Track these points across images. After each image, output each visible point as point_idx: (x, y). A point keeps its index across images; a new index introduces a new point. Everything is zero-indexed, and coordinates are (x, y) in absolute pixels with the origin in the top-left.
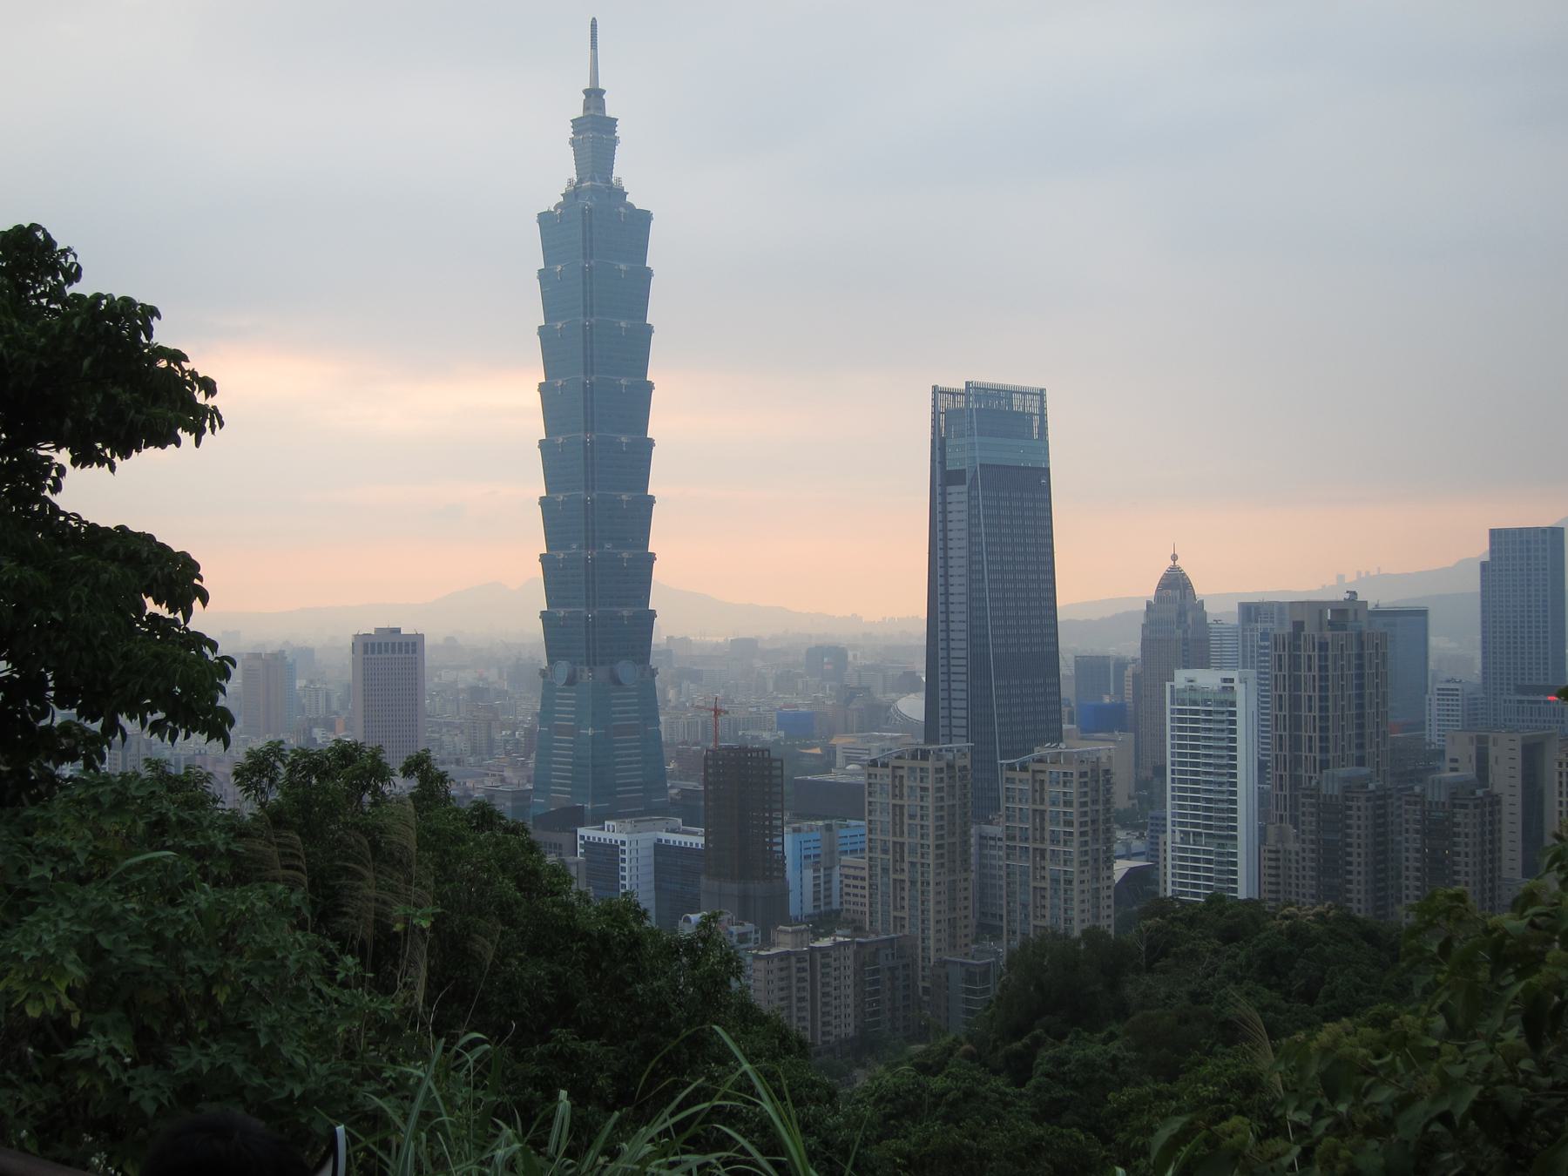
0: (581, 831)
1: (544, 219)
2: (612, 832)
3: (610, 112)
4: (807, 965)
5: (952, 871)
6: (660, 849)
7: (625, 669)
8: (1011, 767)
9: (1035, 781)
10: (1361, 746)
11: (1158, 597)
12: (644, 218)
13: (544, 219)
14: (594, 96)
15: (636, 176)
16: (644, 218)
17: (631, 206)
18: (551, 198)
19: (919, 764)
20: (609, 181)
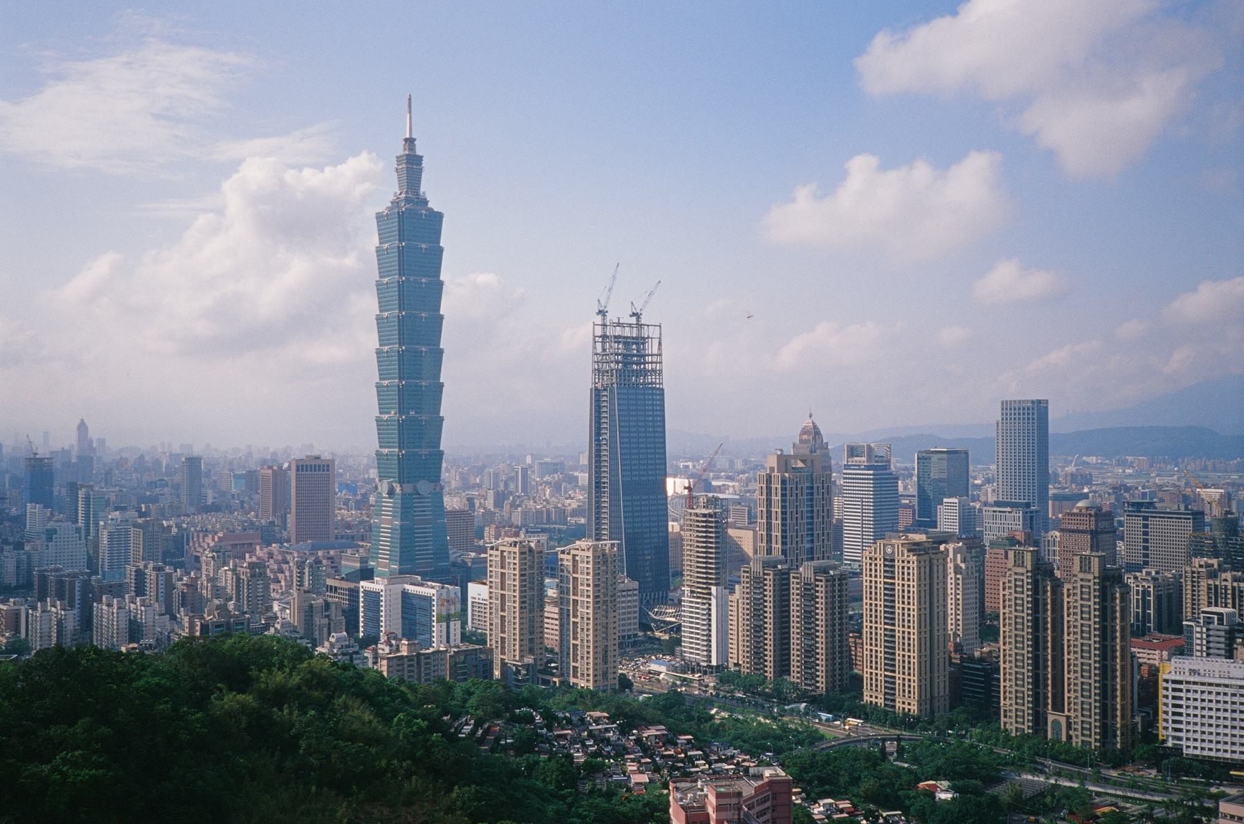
0: (362, 583)
1: (379, 217)
2: (377, 585)
3: (418, 153)
4: (415, 663)
5: (531, 611)
6: (405, 595)
7: (424, 487)
8: (563, 552)
9: (574, 560)
10: (812, 541)
11: (801, 441)
12: (439, 216)
13: (379, 217)
14: (410, 142)
15: (434, 192)
16: (439, 216)
17: (431, 210)
18: (383, 206)
19: (512, 549)
20: (418, 194)
